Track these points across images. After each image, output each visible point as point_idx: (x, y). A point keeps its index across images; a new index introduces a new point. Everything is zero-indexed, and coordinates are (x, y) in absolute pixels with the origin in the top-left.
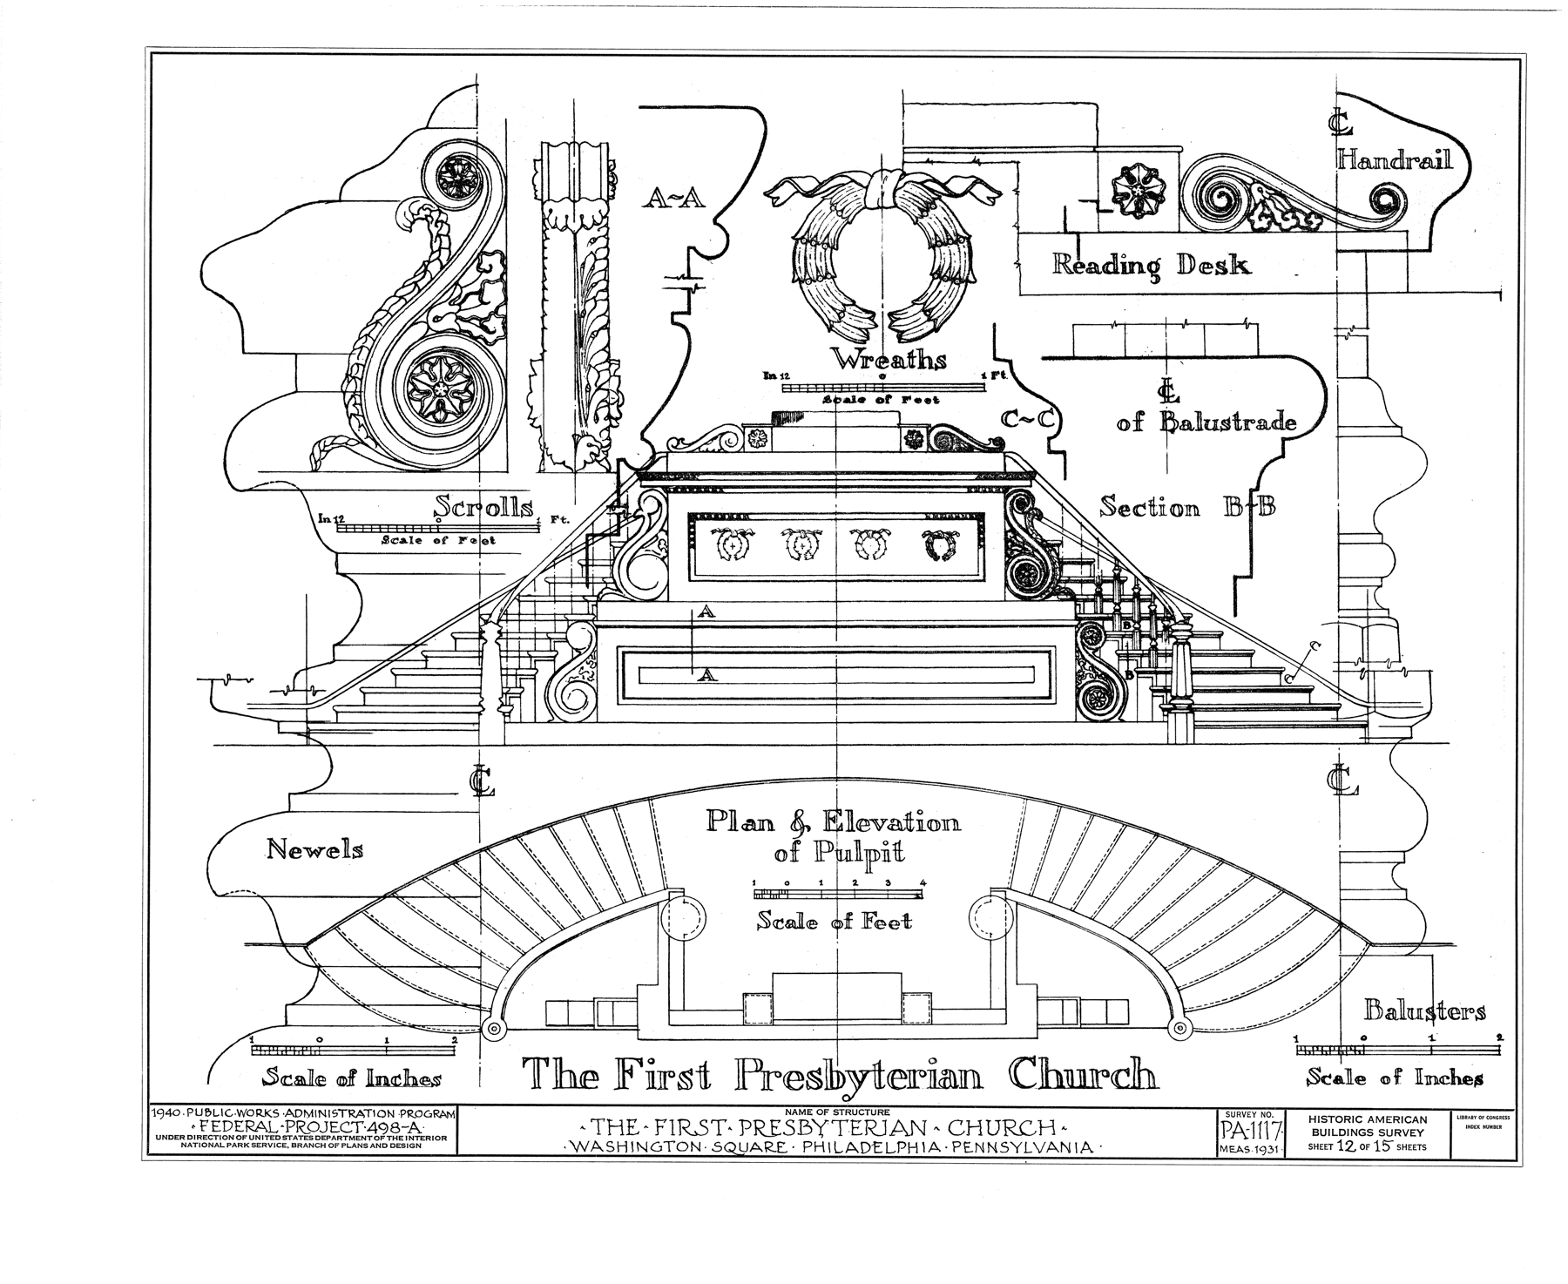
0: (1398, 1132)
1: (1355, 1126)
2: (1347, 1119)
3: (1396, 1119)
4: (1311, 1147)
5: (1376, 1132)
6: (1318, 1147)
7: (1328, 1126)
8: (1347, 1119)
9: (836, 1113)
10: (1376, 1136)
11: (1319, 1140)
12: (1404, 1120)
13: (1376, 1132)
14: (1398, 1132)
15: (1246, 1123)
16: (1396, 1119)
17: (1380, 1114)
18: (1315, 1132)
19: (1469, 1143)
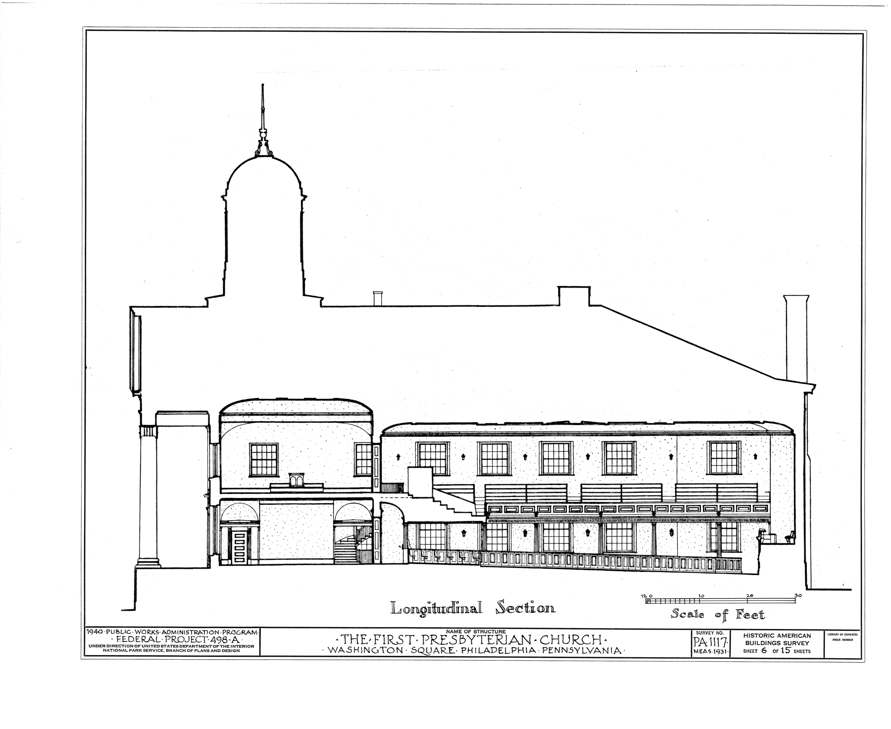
0: (794, 643)
1: (770, 639)
3: (794, 635)
4: (745, 651)
5: (782, 643)
6: (749, 651)
7: (755, 639)
10: (782, 645)
11: (749, 647)
12: (798, 636)
13: (782, 643)
14: (794, 643)
15: (706, 638)
16: (794, 635)
17: (785, 632)
18: (747, 643)
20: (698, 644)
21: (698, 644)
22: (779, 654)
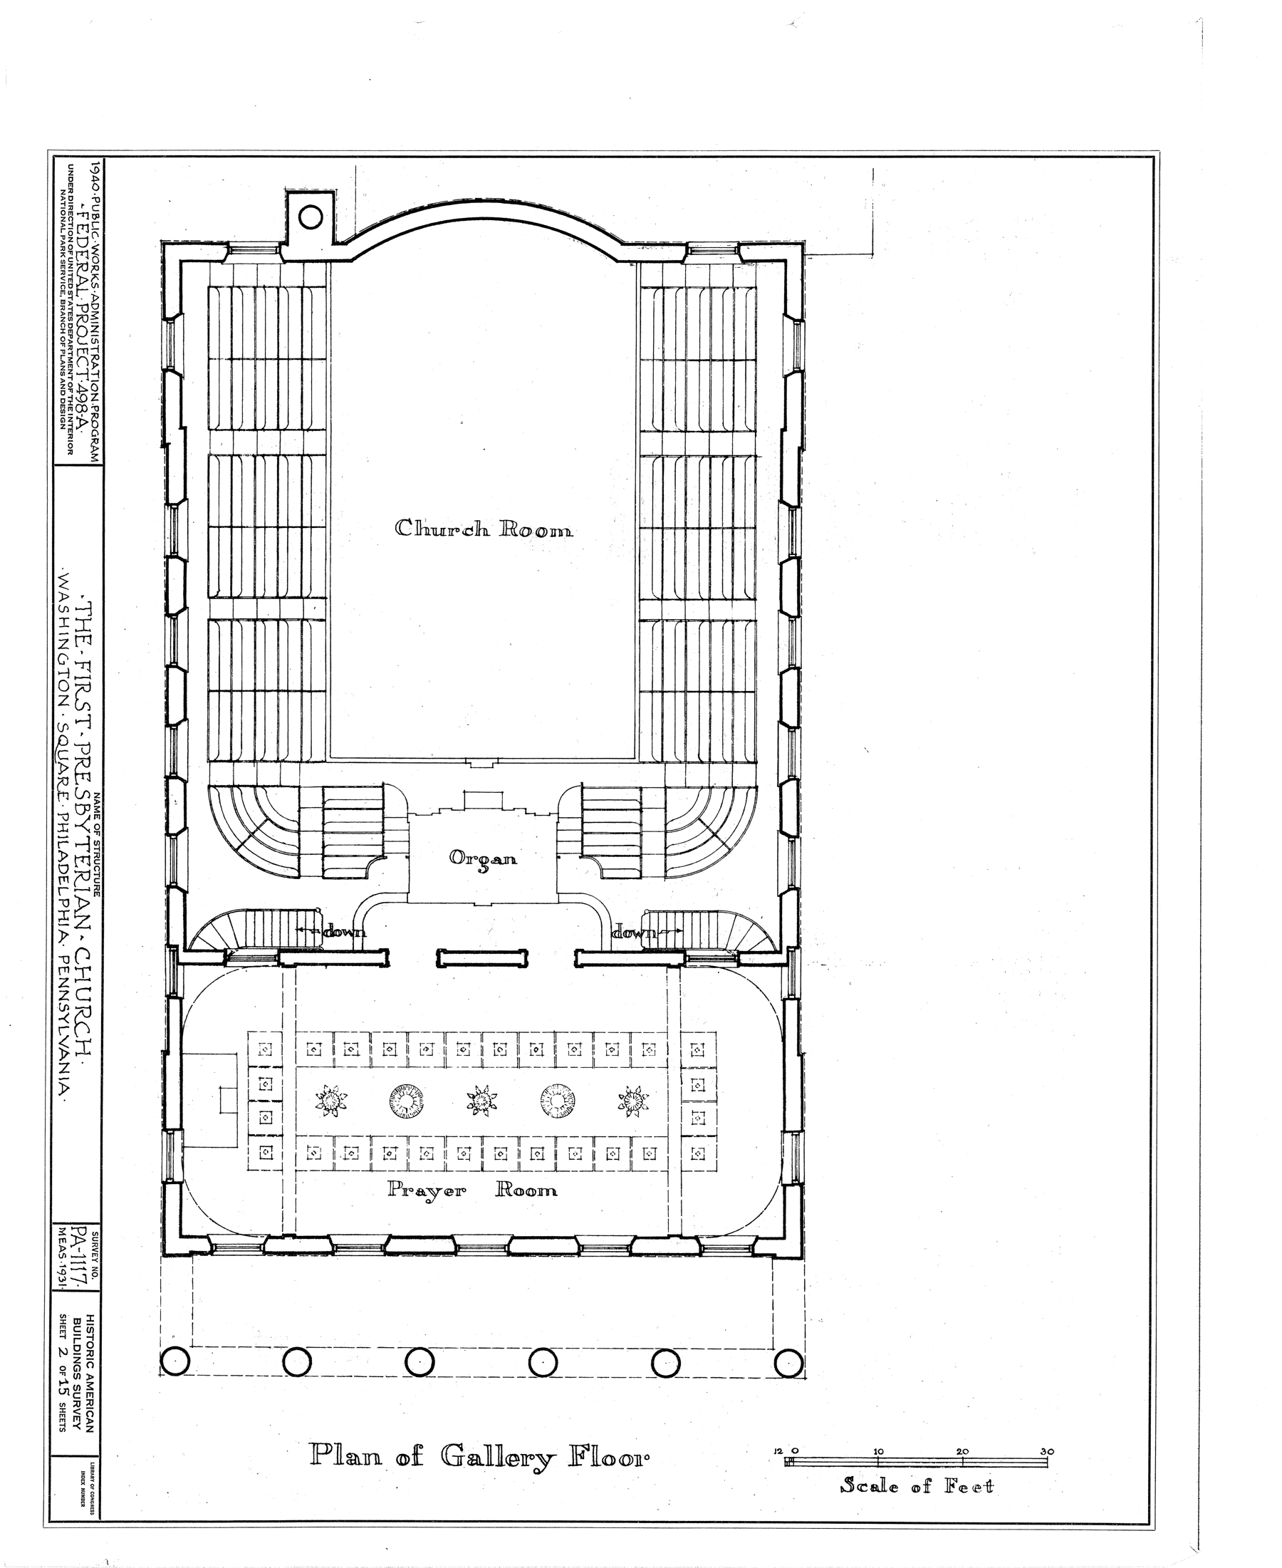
1: (83, 1361)
2: (91, 1353)
3: (91, 1402)
4: (63, 1317)
5: (77, 1382)
6: (63, 1325)
7: (84, 1334)
8: (91, 1353)
9: (96, 843)
10: (73, 1382)
11: (70, 1324)
12: (90, 1410)
13: (77, 1382)
15: (87, 1248)
16: (91, 1402)
17: (96, 1386)
18: (77, 1321)
19: (68, 1473)
20: (75, 1232)
21: (75, 1232)
22: (57, 1376)
